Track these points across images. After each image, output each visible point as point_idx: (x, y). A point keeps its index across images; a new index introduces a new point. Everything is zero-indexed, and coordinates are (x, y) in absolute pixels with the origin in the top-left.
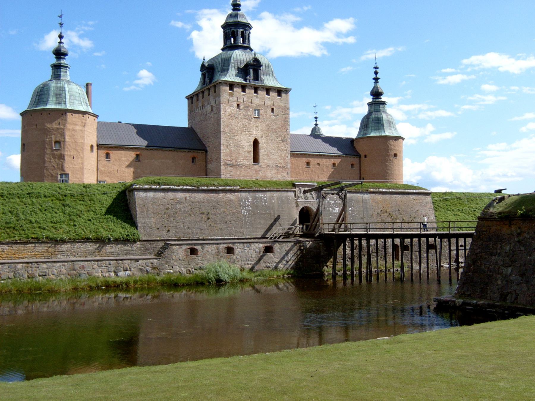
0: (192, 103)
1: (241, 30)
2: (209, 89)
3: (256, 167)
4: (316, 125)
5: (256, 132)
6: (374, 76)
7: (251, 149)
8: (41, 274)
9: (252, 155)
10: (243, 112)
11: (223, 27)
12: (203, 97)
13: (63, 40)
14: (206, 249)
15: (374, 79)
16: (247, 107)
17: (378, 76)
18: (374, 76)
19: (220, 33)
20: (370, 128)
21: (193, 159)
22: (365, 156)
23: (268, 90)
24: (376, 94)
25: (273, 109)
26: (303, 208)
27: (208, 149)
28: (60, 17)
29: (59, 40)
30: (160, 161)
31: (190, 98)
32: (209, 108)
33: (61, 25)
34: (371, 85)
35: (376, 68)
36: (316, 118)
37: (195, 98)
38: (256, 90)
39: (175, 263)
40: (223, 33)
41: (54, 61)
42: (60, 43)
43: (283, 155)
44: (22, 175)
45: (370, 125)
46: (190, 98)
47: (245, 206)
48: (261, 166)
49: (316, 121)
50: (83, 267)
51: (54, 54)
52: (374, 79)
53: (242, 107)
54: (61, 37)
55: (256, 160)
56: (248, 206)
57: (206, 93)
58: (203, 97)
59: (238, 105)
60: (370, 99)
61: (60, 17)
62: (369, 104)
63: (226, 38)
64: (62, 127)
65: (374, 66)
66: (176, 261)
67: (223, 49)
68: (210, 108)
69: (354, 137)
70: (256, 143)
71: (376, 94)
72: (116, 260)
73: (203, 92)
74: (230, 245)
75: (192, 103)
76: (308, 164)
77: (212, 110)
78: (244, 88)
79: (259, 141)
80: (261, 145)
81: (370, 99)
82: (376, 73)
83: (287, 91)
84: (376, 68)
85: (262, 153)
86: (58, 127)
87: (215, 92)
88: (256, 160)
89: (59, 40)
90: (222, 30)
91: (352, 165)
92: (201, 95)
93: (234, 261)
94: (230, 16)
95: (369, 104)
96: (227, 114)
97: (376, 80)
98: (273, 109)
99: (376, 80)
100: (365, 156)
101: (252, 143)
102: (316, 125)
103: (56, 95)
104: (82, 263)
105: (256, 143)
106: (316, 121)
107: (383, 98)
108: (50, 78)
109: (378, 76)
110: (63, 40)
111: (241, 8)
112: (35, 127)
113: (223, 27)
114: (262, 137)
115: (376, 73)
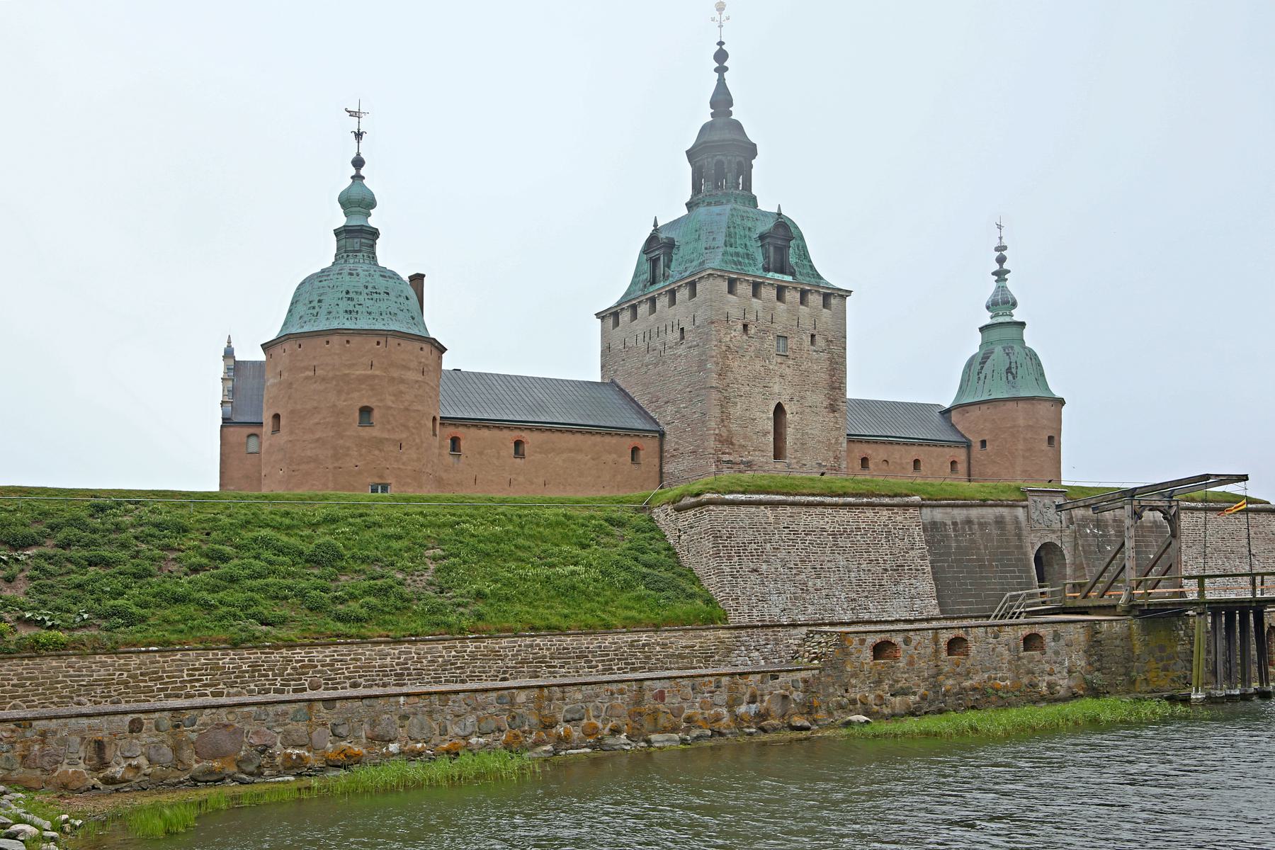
2: (672, 293)
6: (996, 267)
8: (569, 717)
10: (756, 343)
12: (653, 309)
13: (363, 172)
14: (914, 643)
15: (994, 274)
16: (765, 332)
17: (1006, 266)
18: (996, 267)
25: (813, 336)
26: (1044, 546)
29: (353, 171)
30: (565, 456)
32: (674, 336)
33: (359, 135)
34: (991, 284)
38: (781, 290)
39: (853, 681)
41: (341, 220)
42: (358, 178)
48: (789, 466)
50: (661, 696)
52: (994, 274)
53: (752, 331)
54: (358, 163)
57: (663, 302)
58: (653, 309)
59: (745, 326)
60: (986, 318)
64: (377, 373)
66: (855, 675)
67: (689, 205)
72: (732, 675)
74: (961, 633)
77: (682, 338)
78: (756, 287)
82: (1001, 260)
83: (844, 294)
86: (370, 372)
87: (693, 294)
89: (353, 171)
93: (969, 673)
96: (724, 348)
97: (1001, 275)
99: (1001, 275)
104: (658, 685)
107: (1017, 315)
108: (328, 261)
109: (1006, 266)
110: (363, 172)
112: (311, 373)
115: (1001, 260)
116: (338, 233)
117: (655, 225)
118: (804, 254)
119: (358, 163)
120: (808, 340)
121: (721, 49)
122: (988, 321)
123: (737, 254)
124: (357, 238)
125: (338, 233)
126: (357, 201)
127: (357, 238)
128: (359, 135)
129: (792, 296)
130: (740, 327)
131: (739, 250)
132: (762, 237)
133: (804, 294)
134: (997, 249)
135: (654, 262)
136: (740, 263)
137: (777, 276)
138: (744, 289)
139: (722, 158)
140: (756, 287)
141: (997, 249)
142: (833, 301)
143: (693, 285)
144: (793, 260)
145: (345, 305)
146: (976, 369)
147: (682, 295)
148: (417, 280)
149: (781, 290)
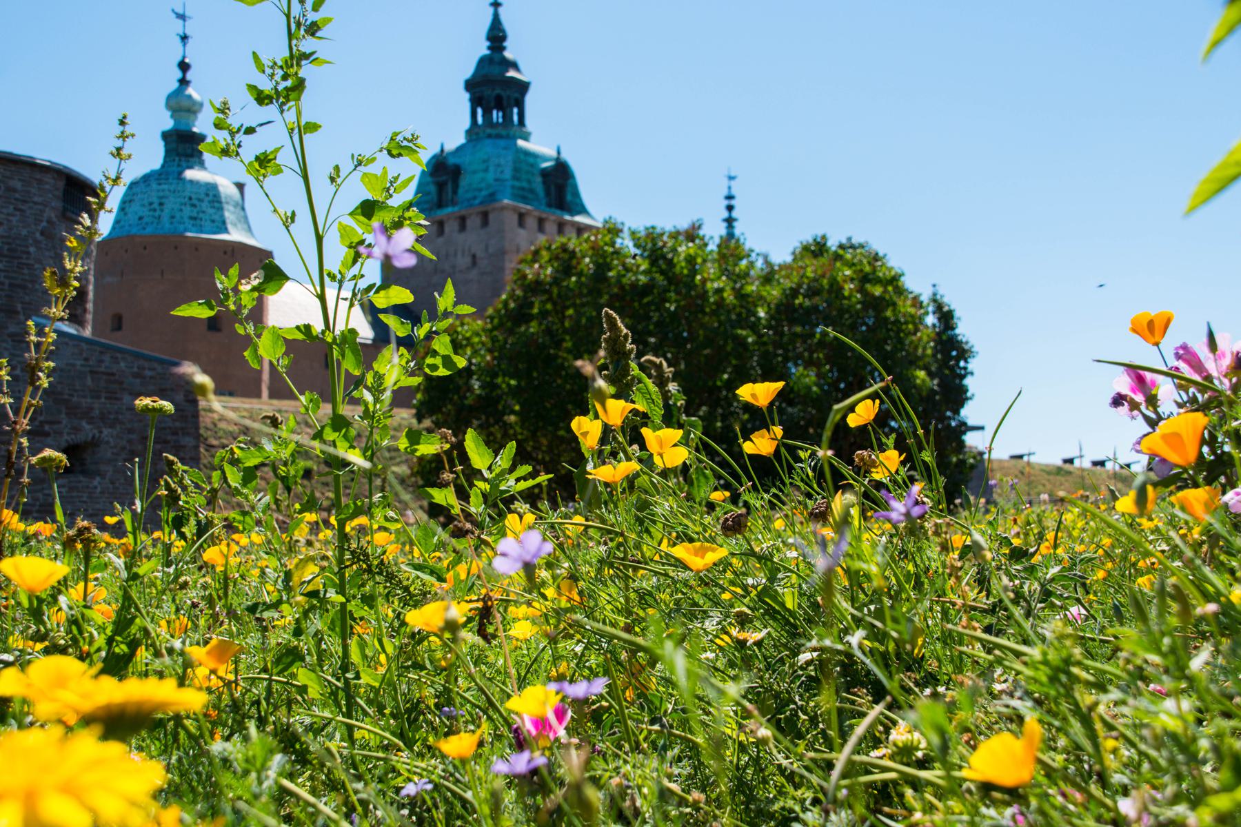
2: (463, 220)
17: (735, 214)
29: (179, 75)
33: (184, 38)
35: (730, 197)
41: (169, 124)
42: (184, 82)
54: (184, 66)
65: (725, 192)
68: (468, 260)
82: (730, 208)
84: (730, 197)
97: (730, 221)
99: (730, 221)
110: (189, 76)
115: (730, 208)
116: (166, 136)
118: (576, 194)
125: (166, 136)
128: (184, 38)
135: (441, 187)
144: (569, 197)
145: (188, 211)
147: (474, 222)
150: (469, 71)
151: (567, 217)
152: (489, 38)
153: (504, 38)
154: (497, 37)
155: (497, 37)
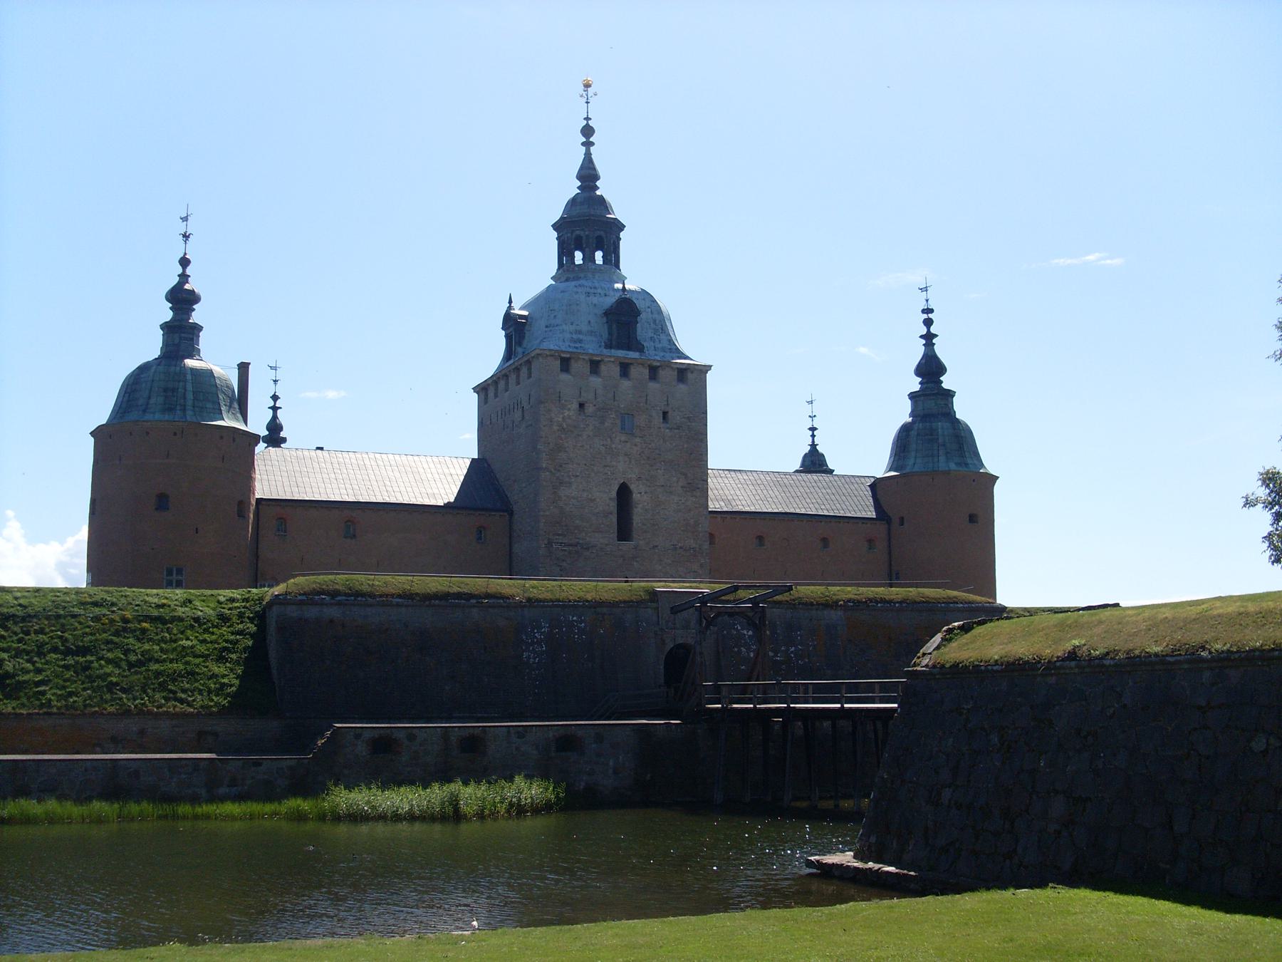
0: (486, 402)
1: (598, 233)
2: (517, 369)
3: (626, 545)
4: (813, 446)
5: (624, 470)
7: (613, 506)
9: (615, 520)
11: (556, 227)
17: (933, 330)
19: (550, 242)
20: (913, 454)
21: (480, 530)
22: (902, 520)
23: (653, 371)
24: (930, 369)
25: (665, 414)
27: (515, 508)
28: (185, 219)
31: (482, 390)
32: (517, 415)
33: (186, 236)
34: (919, 351)
35: (928, 311)
36: (813, 429)
37: (491, 393)
38: (625, 368)
39: (346, 772)
40: (555, 245)
43: (692, 522)
44: (90, 568)
45: (913, 446)
46: (482, 390)
47: (533, 643)
49: (813, 436)
51: (168, 300)
53: (590, 409)
54: (185, 262)
55: (624, 532)
56: (539, 643)
57: (513, 377)
59: (581, 405)
61: (185, 219)
62: (913, 396)
63: (565, 251)
69: (879, 475)
70: (624, 493)
71: (930, 369)
73: (506, 376)
74: (477, 732)
75: (486, 402)
76: (760, 539)
78: (595, 366)
79: (632, 487)
80: (636, 496)
81: (915, 384)
82: (928, 323)
83: (702, 371)
84: (928, 311)
85: (638, 517)
88: (624, 532)
89: (180, 271)
90: (555, 234)
91: (870, 541)
92: (502, 384)
94: (573, 202)
95: (913, 396)
96: (555, 428)
97: (929, 338)
98: (665, 414)
99: (929, 338)
100: (902, 520)
101: (614, 494)
102: (813, 446)
103: (165, 390)
105: (624, 493)
106: (813, 436)
109: (933, 330)
110: (188, 271)
111: (598, 183)
113: (556, 227)
114: (639, 478)
115: (928, 323)
117: (510, 302)
119: (185, 262)
120: (658, 419)
121: (587, 125)
122: (917, 387)
123: (580, 332)
124: (181, 336)
126: (182, 299)
127: (181, 336)
128: (186, 236)
129: (639, 373)
130: (575, 406)
131: (584, 328)
132: (607, 313)
133: (653, 371)
134: (924, 311)
136: (580, 341)
137: (621, 353)
138: (579, 367)
139: (588, 228)
140: (595, 366)
141: (924, 311)
142: (690, 376)
143: (529, 362)
146: (904, 442)
147: (524, 370)
148: (244, 368)
149: (625, 368)
150: (557, 214)
151: (634, 355)
152: (579, 177)
153: (597, 177)
154: (588, 175)
155: (588, 175)
